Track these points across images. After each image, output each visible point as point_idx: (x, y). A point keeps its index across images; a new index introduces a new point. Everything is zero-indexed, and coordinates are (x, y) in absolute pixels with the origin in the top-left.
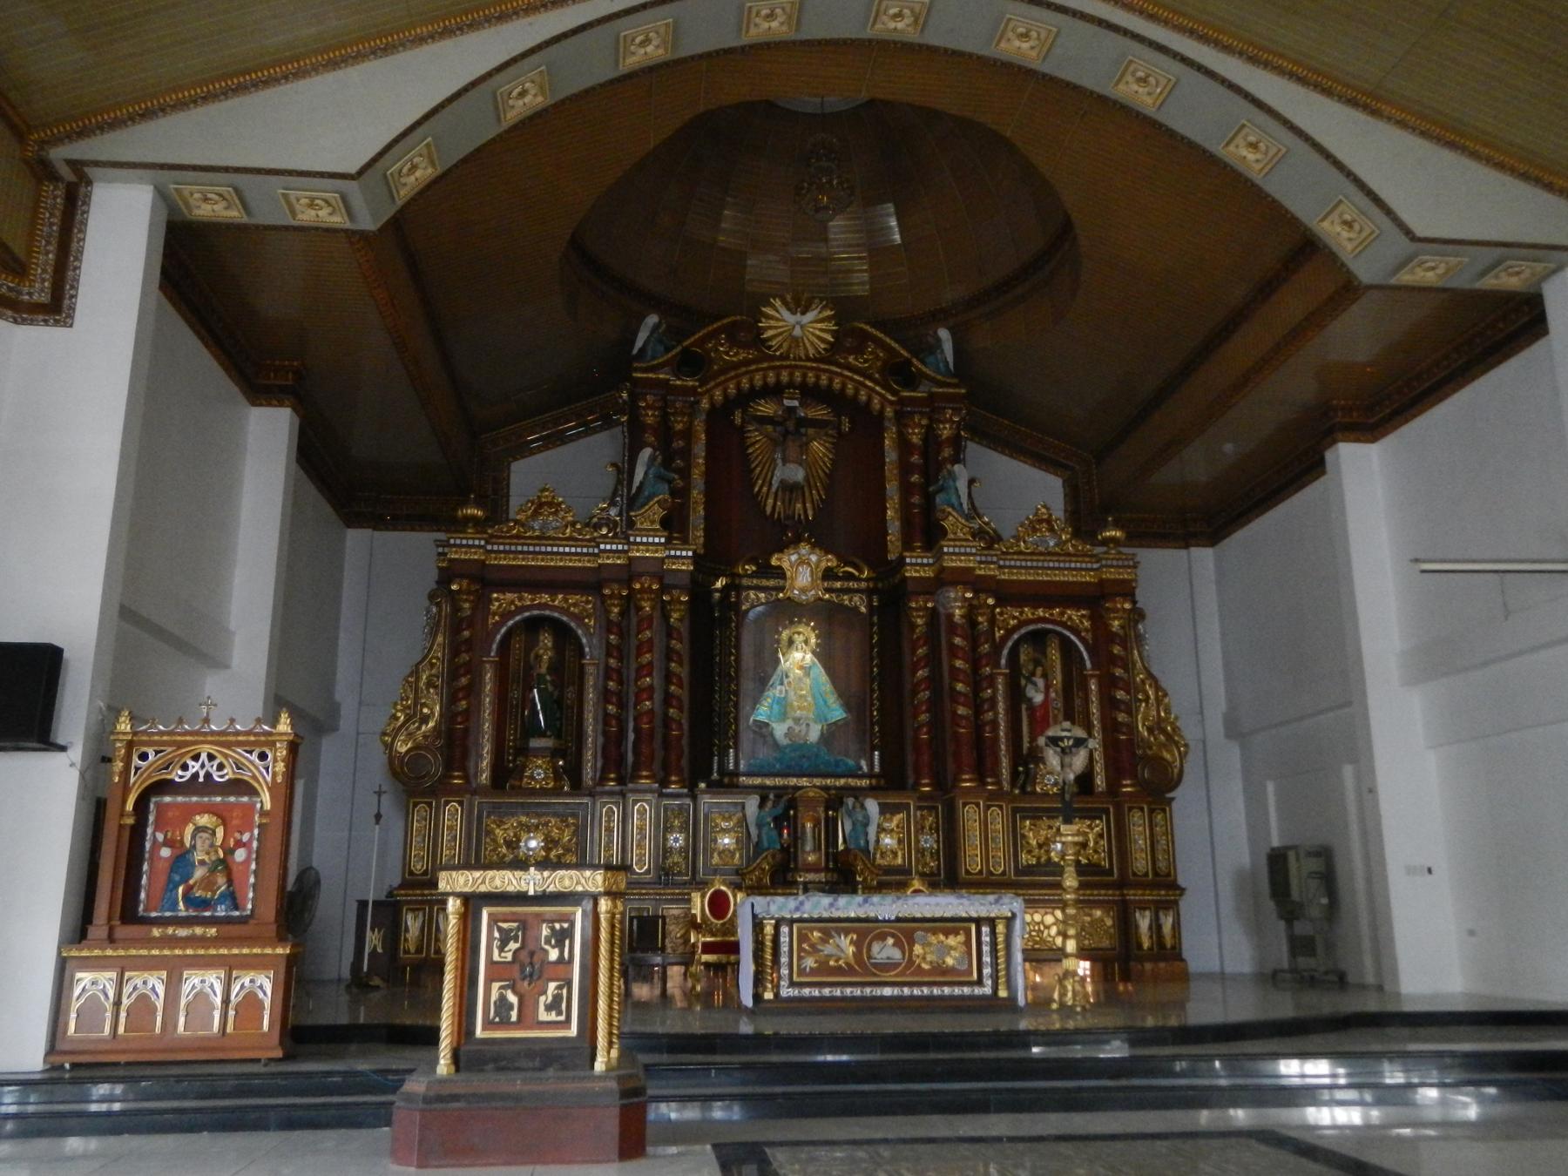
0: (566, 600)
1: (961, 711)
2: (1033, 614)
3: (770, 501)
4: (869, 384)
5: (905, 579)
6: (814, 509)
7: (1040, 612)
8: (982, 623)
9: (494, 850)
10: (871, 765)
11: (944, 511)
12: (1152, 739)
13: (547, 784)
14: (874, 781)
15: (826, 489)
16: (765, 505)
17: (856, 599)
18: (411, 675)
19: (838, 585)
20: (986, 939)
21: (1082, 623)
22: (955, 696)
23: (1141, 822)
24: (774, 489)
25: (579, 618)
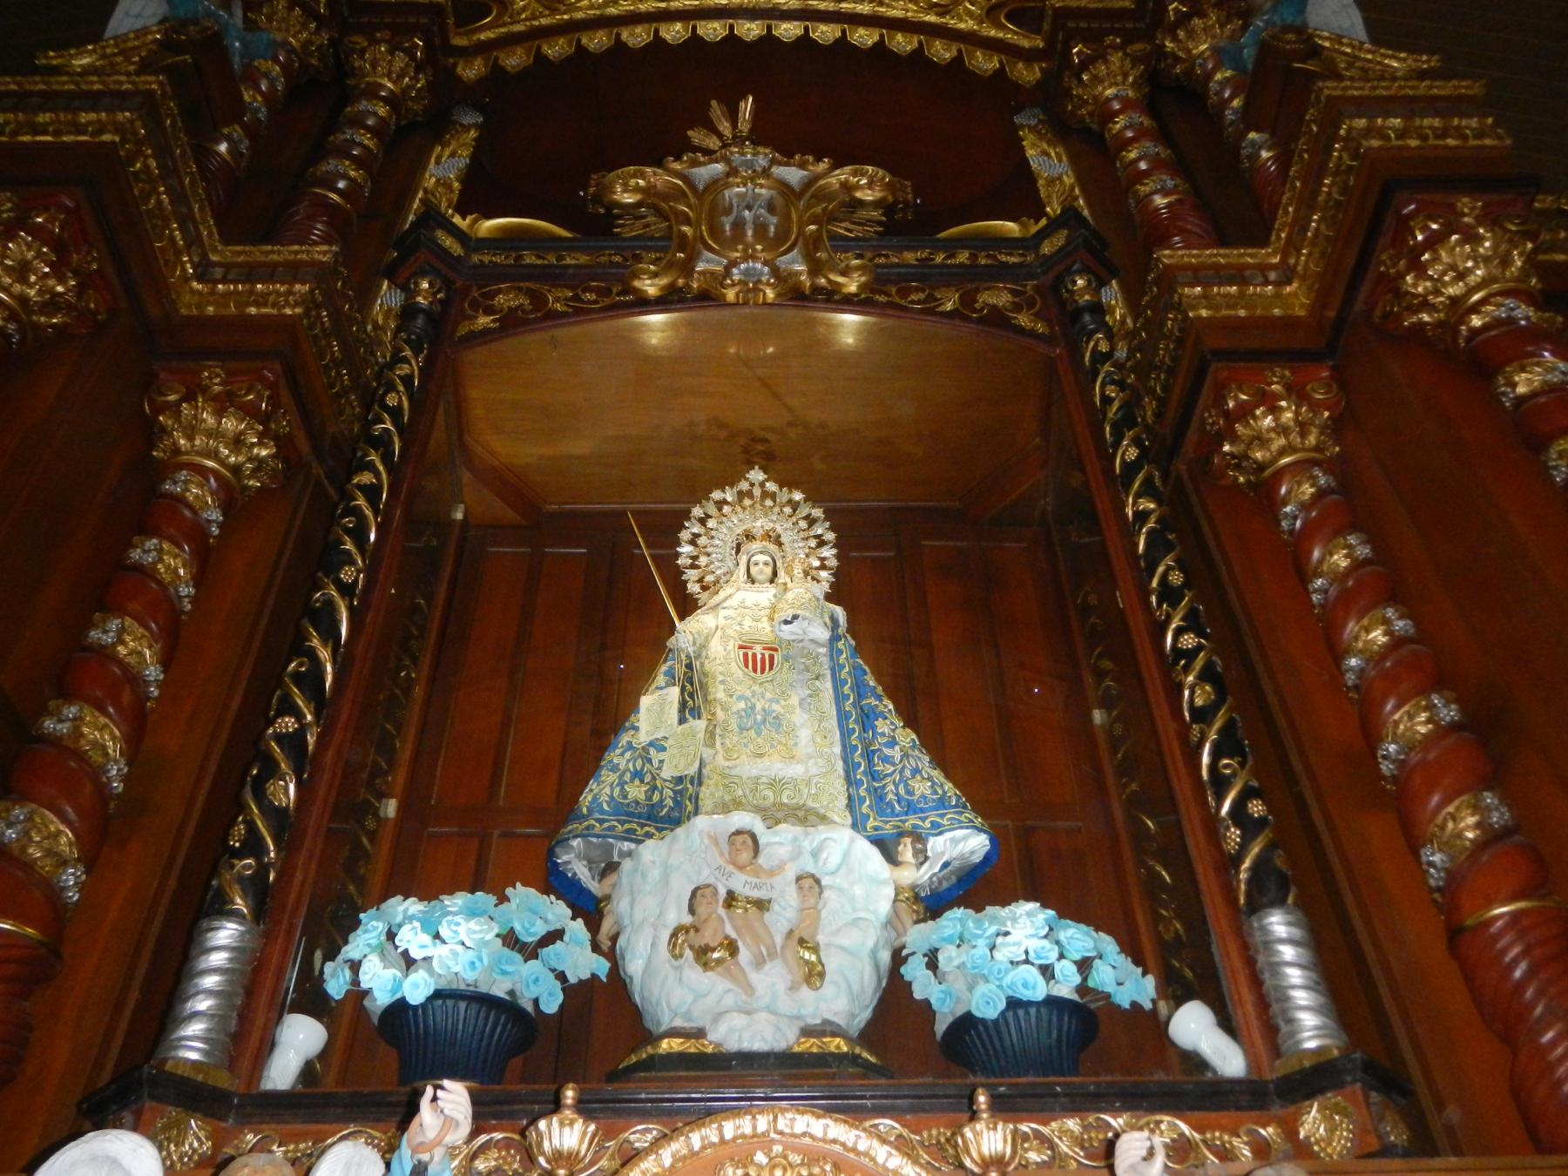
17: (997, 297)
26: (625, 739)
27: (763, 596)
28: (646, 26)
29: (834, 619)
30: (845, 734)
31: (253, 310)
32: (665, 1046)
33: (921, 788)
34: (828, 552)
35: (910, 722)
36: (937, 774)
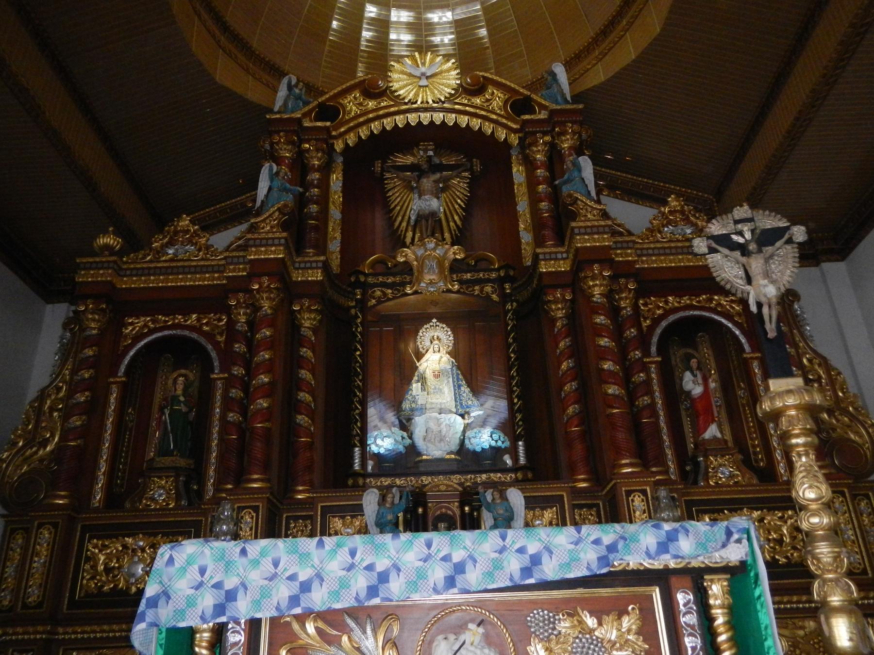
0: (199, 320)
1: (612, 390)
2: (679, 302)
3: (410, 234)
4: (494, 117)
5: (542, 273)
6: (452, 237)
7: (686, 300)
8: (625, 308)
9: (93, 578)
10: (515, 459)
11: (570, 196)
12: (834, 421)
13: (168, 504)
14: (520, 475)
15: (463, 219)
16: (405, 237)
17: (488, 289)
18: (34, 401)
19: (468, 276)
20: (689, 619)
21: (733, 308)
22: (605, 377)
23: (845, 508)
24: (412, 222)
25: (210, 336)
26: (410, 392)
27: (437, 356)
28: (391, 118)
29: (453, 362)
30: (455, 390)
31: (310, 279)
32: (424, 457)
33: (470, 403)
34: (451, 338)
35: (468, 386)
36: (473, 399)
